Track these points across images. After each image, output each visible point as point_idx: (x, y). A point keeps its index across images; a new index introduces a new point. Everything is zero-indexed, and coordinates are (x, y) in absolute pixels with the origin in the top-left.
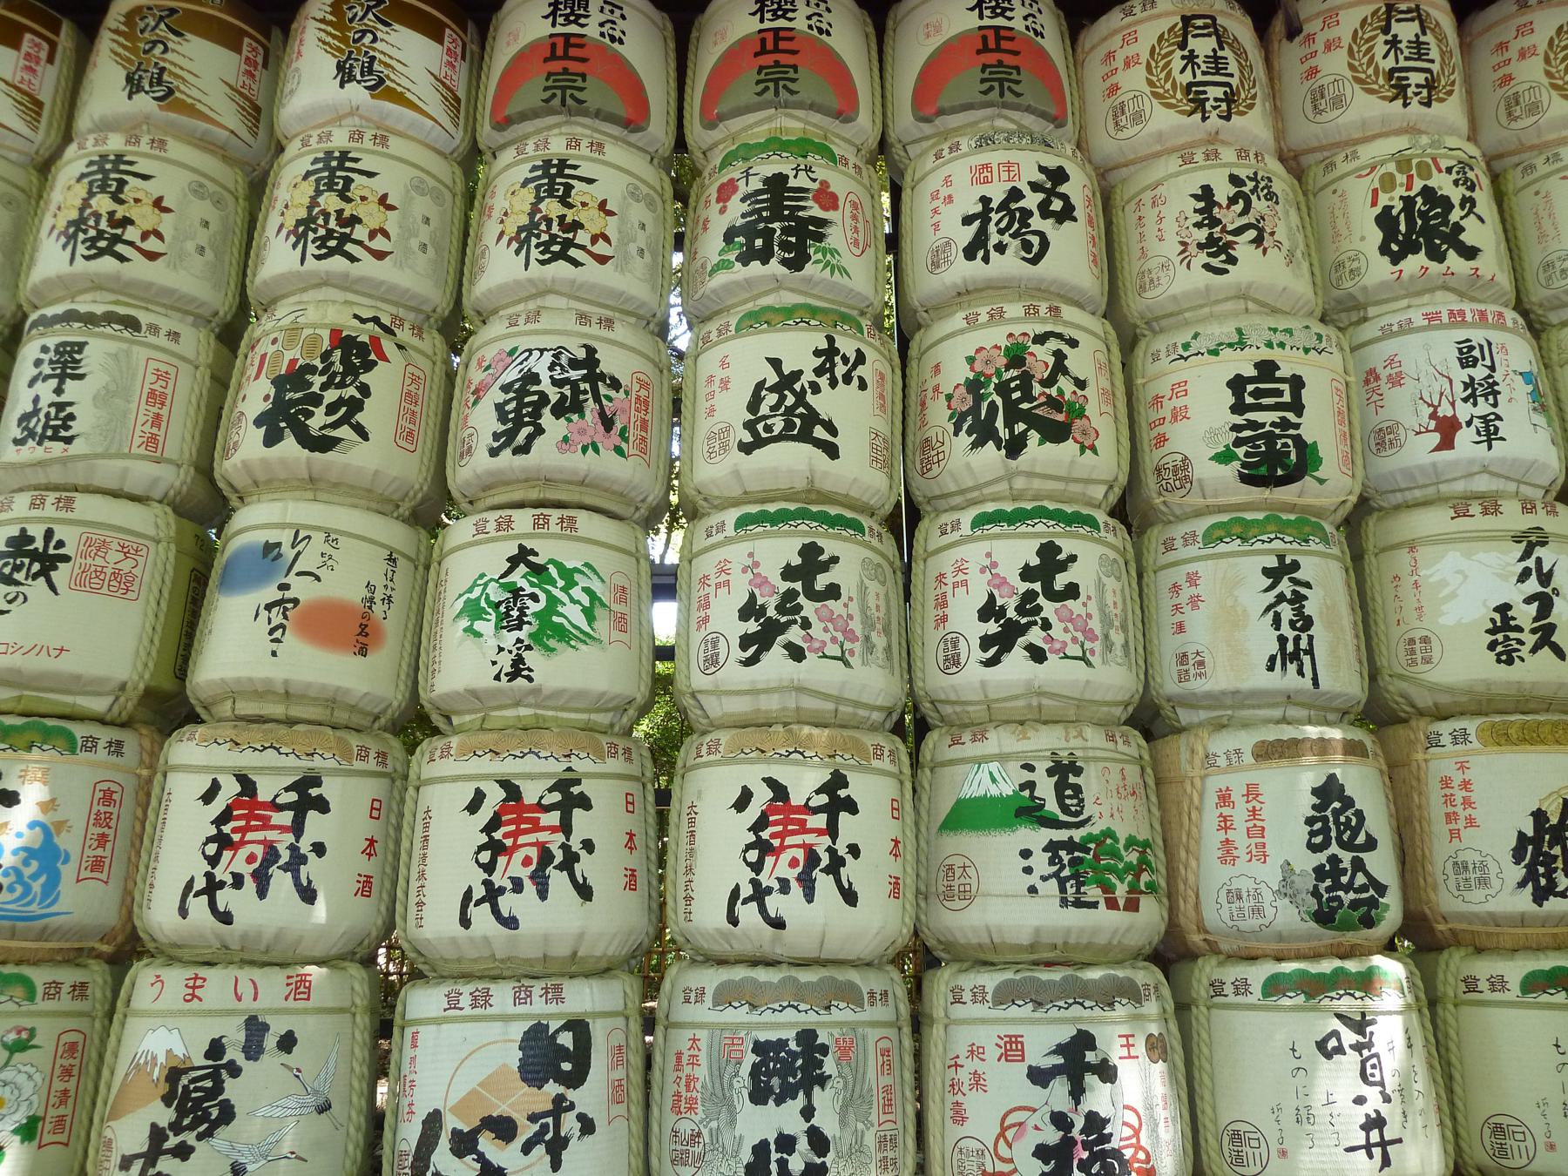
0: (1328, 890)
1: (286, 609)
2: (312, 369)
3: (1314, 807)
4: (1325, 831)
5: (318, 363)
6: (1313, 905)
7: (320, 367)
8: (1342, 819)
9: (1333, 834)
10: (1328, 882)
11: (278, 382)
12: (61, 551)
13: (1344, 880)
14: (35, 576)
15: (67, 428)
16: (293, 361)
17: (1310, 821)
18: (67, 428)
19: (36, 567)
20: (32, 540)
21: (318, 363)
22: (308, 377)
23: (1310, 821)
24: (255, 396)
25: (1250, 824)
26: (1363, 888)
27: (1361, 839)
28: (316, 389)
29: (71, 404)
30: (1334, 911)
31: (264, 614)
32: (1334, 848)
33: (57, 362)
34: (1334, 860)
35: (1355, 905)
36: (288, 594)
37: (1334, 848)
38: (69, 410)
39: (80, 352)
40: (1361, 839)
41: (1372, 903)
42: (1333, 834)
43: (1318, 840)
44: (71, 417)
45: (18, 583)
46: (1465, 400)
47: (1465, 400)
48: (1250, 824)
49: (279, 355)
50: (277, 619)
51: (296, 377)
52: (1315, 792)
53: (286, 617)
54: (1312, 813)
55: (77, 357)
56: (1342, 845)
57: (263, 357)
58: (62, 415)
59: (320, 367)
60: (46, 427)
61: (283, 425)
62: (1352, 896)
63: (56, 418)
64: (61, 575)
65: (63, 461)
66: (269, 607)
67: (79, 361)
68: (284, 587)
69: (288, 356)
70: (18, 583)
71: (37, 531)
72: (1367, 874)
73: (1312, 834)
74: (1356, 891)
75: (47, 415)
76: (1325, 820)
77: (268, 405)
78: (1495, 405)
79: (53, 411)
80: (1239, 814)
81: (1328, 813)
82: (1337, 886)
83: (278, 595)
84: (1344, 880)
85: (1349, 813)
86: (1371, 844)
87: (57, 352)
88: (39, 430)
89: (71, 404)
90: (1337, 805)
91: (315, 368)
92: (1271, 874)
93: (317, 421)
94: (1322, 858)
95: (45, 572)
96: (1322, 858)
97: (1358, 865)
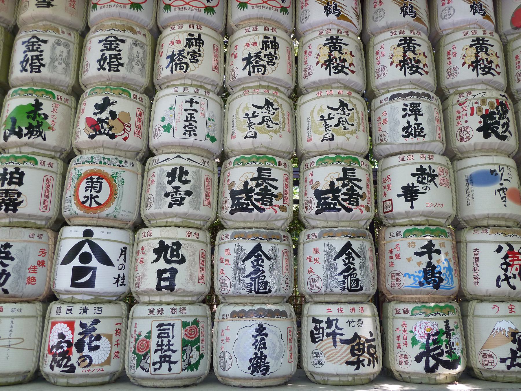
1: (504, 192)
12: (435, 173)
14: (430, 181)
15: (423, 132)
18: (423, 132)
19: (430, 178)
20: (425, 170)
22: (494, 115)
28: (497, 119)
29: (421, 124)
31: (498, 193)
36: (504, 187)
38: (421, 126)
44: (422, 128)
45: (426, 184)
50: (503, 195)
53: (505, 194)
58: (420, 128)
60: (415, 132)
63: (418, 129)
64: (437, 180)
65: (423, 143)
66: (499, 191)
68: (501, 184)
70: (426, 184)
71: (426, 166)
75: (415, 127)
79: (416, 126)
83: (500, 187)
88: (413, 132)
89: (421, 124)
95: (433, 180)
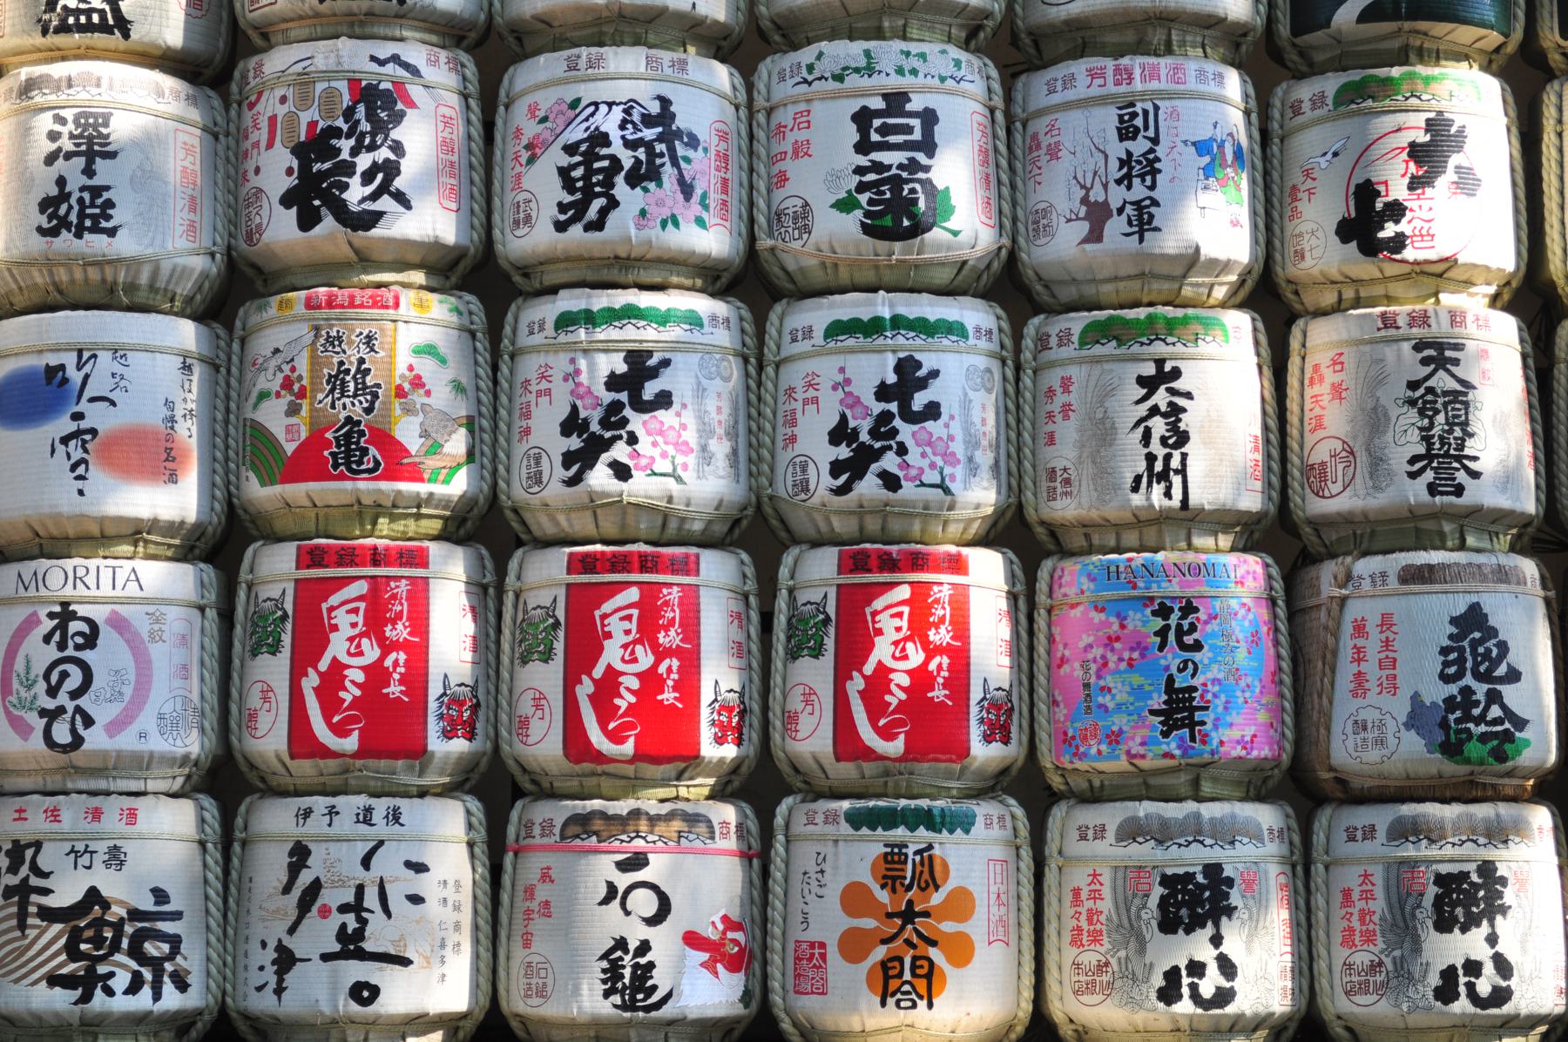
0: (1457, 721)
2: (336, 133)
3: (1451, 637)
4: (1461, 661)
5: (340, 123)
6: (1441, 737)
7: (345, 127)
8: (1481, 650)
9: (1469, 664)
10: (1458, 714)
11: (299, 151)
13: (1476, 712)
16: (312, 125)
17: (1445, 651)
21: (340, 123)
22: (334, 142)
23: (1445, 651)
24: (275, 170)
25: (1383, 655)
26: (1496, 722)
27: (1502, 670)
28: (345, 155)
30: (1461, 743)
32: (1468, 680)
33: (81, 136)
34: (1467, 692)
35: (1484, 738)
37: (1468, 680)
39: (106, 125)
40: (1502, 670)
41: (1507, 737)
42: (1469, 664)
43: (1452, 670)
46: (1119, 182)
47: (1119, 182)
48: (1383, 655)
49: (292, 118)
51: (317, 146)
52: (1454, 621)
54: (1446, 642)
55: (104, 131)
56: (1478, 677)
57: (273, 120)
59: (345, 127)
61: (317, 203)
62: (1483, 728)
67: (108, 136)
69: (305, 117)
72: (1504, 707)
73: (1446, 664)
74: (1489, 724)
76: (1461, 650)
77: (292, 181)
78: (1153, 187)
80: (1372, 645)
81: (1466, 643)
82: (1467, 717)
84: (1476, 712)
85: (1490, 644)
86: (1514, 676)
87: (77, 123)
90: (1477, 635)
91: (340, 129)
92: (1400, 708)
93: (355, 193)
94: (1453, 689)
96: (1453, 689)
97: (1494, 697)
